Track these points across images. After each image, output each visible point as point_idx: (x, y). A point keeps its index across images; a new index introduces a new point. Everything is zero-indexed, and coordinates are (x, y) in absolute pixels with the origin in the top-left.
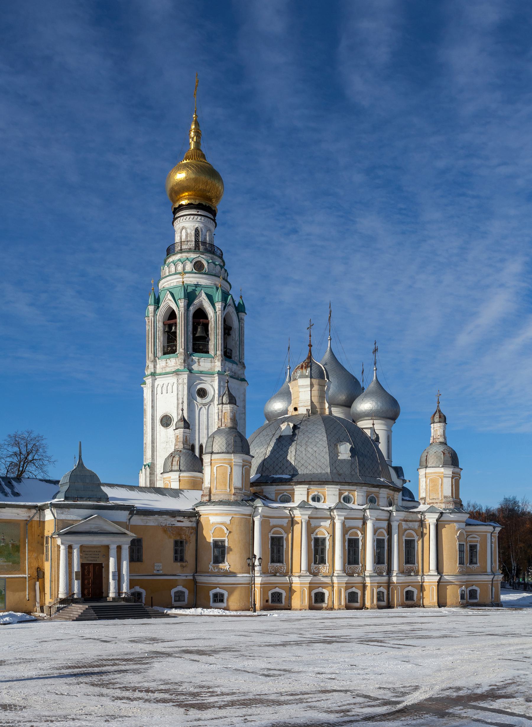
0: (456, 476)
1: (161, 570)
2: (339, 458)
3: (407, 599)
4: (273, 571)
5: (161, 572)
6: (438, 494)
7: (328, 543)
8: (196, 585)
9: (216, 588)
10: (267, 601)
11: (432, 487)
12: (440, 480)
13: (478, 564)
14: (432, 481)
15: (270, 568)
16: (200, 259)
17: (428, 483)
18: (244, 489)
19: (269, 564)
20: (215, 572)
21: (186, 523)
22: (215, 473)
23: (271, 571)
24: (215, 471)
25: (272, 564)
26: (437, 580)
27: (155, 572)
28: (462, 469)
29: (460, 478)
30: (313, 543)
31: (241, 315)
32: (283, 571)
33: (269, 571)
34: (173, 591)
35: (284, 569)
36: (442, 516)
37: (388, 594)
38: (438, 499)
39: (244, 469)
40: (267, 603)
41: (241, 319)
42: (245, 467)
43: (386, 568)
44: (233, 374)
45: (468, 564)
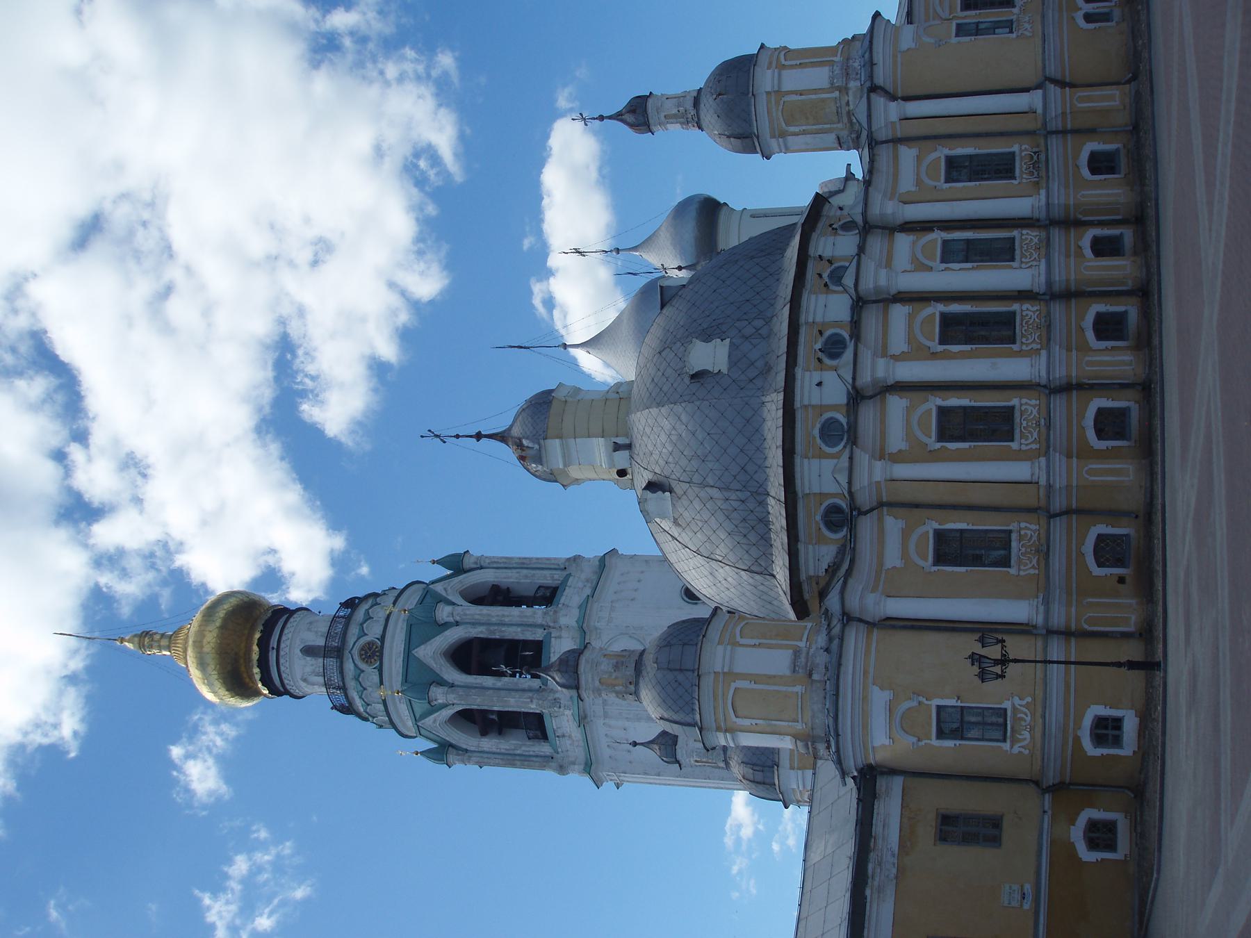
0: (778, 58)
1: (1022, 886)
2: (725, 371)
3: (1112, 170)
4: (1034, 561)
5: (1028, 888)
6: (823, 100)
8: (1070, 784)
9: (1077, 740)
10: (1121, 580)
11: (807, 118)
12: (787, 98)
15: (1024, 570)
17: (797, 129)
18: (798, 643)
19: (1013, 571)
20: (1032, 738)
21: (890, 810)
22: (754, 722)
23: (1033, 567)
24: (747, 722)
25: (1013, 562)
26: (1058, 90)
27: (1026, 906)
28: (762, 46)
29: (785, 48)
30: (953, 446)
31: (468, 563)
32: (1034, 531)
33: (1032, 572)
34: (1086, 855)
35: (1026, 528)
36: (882, 89)
37: (1101, 224)
39: (743, 641)
40: (1128, 580)
41: (476, 563)
42: (738, 638)
43: (1024, 232)
44: (589, 585)
45: (1013, 10)
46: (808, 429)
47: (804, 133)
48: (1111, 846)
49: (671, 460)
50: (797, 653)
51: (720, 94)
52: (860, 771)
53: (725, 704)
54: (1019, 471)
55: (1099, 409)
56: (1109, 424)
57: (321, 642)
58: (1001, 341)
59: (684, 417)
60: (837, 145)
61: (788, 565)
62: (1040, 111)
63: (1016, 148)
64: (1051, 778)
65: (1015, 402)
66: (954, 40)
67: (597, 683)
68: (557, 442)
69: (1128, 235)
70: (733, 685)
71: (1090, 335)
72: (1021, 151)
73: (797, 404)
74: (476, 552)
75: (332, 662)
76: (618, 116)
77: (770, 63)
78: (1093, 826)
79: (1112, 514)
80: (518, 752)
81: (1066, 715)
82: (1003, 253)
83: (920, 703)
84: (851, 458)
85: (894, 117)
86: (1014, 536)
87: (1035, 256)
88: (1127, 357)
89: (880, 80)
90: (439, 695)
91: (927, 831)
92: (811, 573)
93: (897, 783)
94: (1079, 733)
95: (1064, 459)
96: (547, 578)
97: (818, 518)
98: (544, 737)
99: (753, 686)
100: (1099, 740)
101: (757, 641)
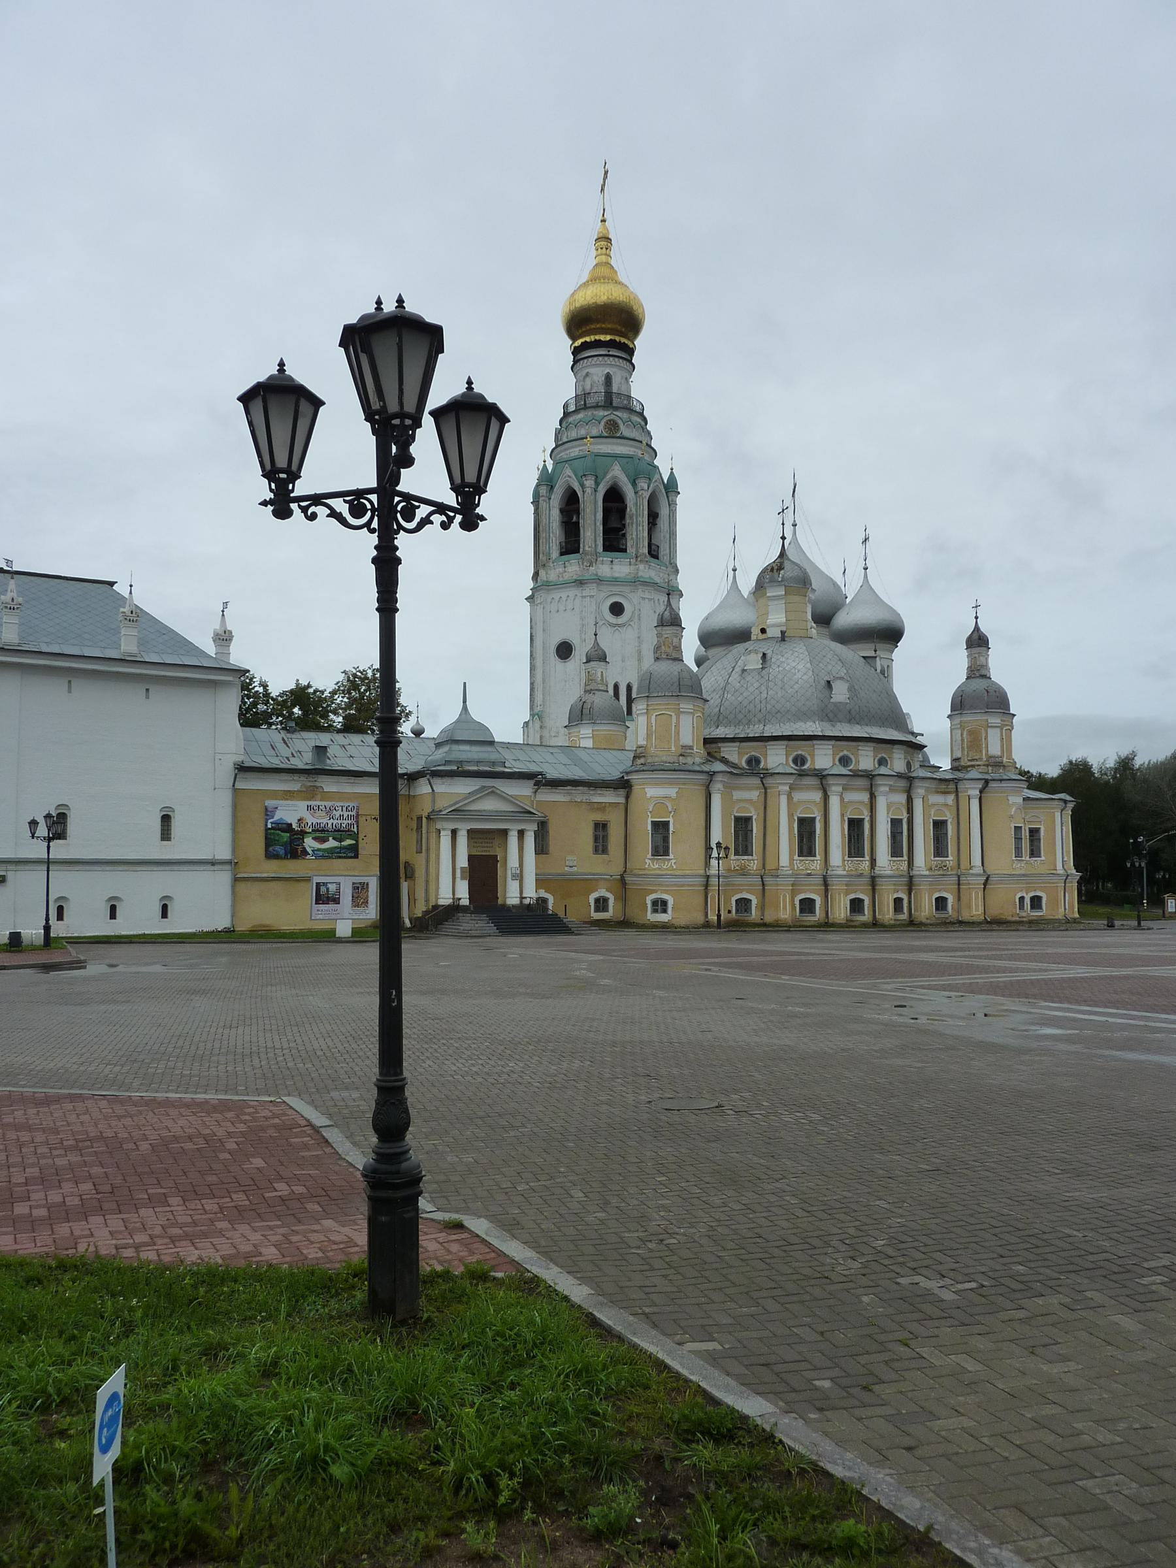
0: (1007, 725)
2: (832, 700)
3: (937, 909)
6: (981, 751)
7: (819, 827)
10: (730, 912)
11: (971, 742)
13: (1043, 858)
14: (970, 733)
16: (612, 417)
17: (965, 736)
20: (655, 869)
22: (654, 725)
24: (653, 721)
28: (1014, 715)
29: (1013, 728)
30: (796, 825)
37: (910, 902)
38: (981, 759)
39: (695, 717)
46: (801, 749)
47: (962, 740)
48: (597, 910)
49: (781, 669)
50: (691, 748)
51: (988, 692)
52: (628, 781)
53: (661, 710)
54: (784, 860)
55: (815, 900)
56: (807, 905)
57: (615, 389)
58: (849, 851)
59: (805, 677)
60: (954, 757)
61: (727, 736)
62: (971, 871)
63: (950, 858)
64: (628, 879)
65: (818, 857)
66: (1013, 826)
67: (666, 636)
68: (784, 593)
69: (904, 916)
70: (673, 714)
71: (853, 896)
72: (949, 861)
73: (815, 742)
74: (679, 500)
75: (601, 398)
76: (977, 628)
77: (1004, 721)
78: (605, 900)
79: (762, 907)
80: (551, 535)
81: (667, 886)
82: (896, 851)
83: (671, 812)
84: (792, 774)
85: (971, 792)
86: (750, 857)
87: (894, 868)
88: (843, 915)
89: (992, 784)
90: (589, 483)
91: (599, 817)
92: (722, 749)
93: (622, 800)
94: (659, 892)
95: (792, 882)
96: (664, 551)
97: (753, 753)
98: (562, 554)
99: (674, 725)
100: (655, 903)
101: (695, 725)
